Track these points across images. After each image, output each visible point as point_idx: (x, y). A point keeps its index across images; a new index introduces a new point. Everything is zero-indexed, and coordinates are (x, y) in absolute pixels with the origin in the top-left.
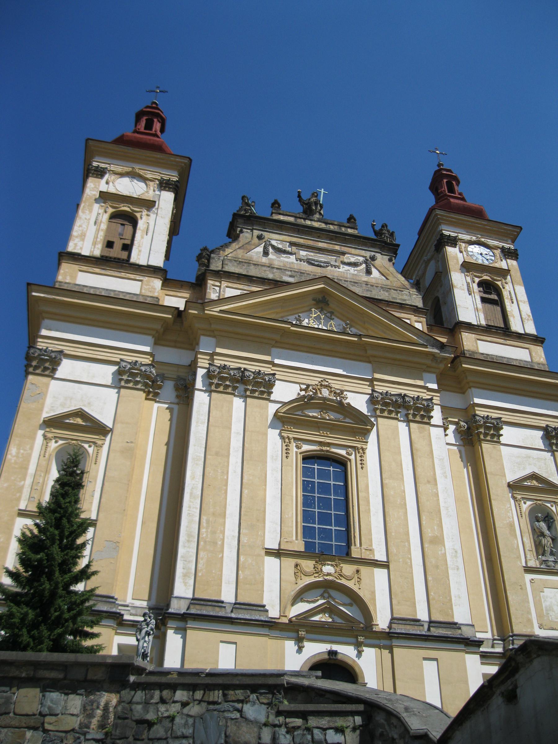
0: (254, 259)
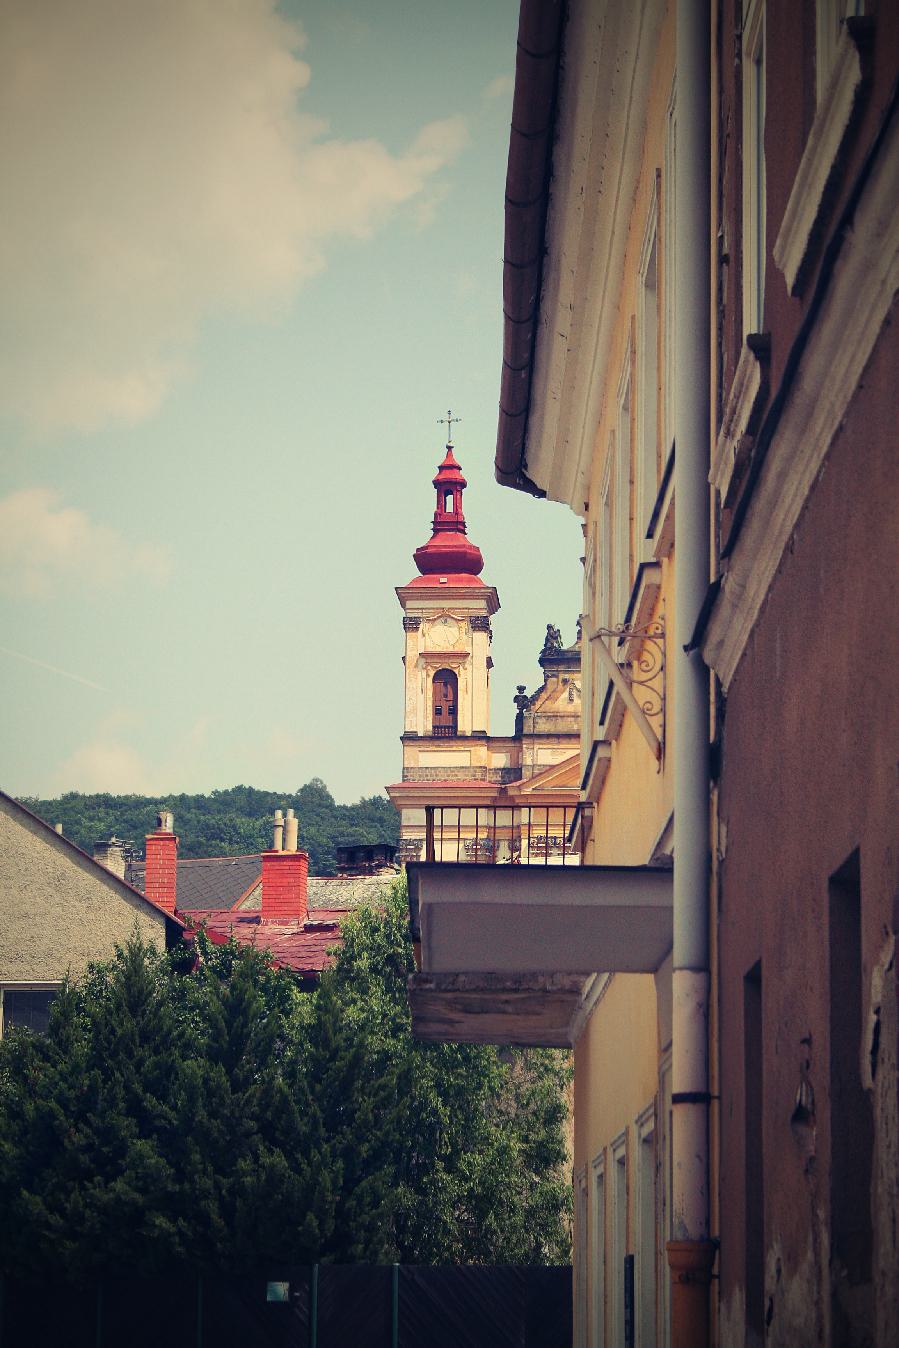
0: (561, 710)
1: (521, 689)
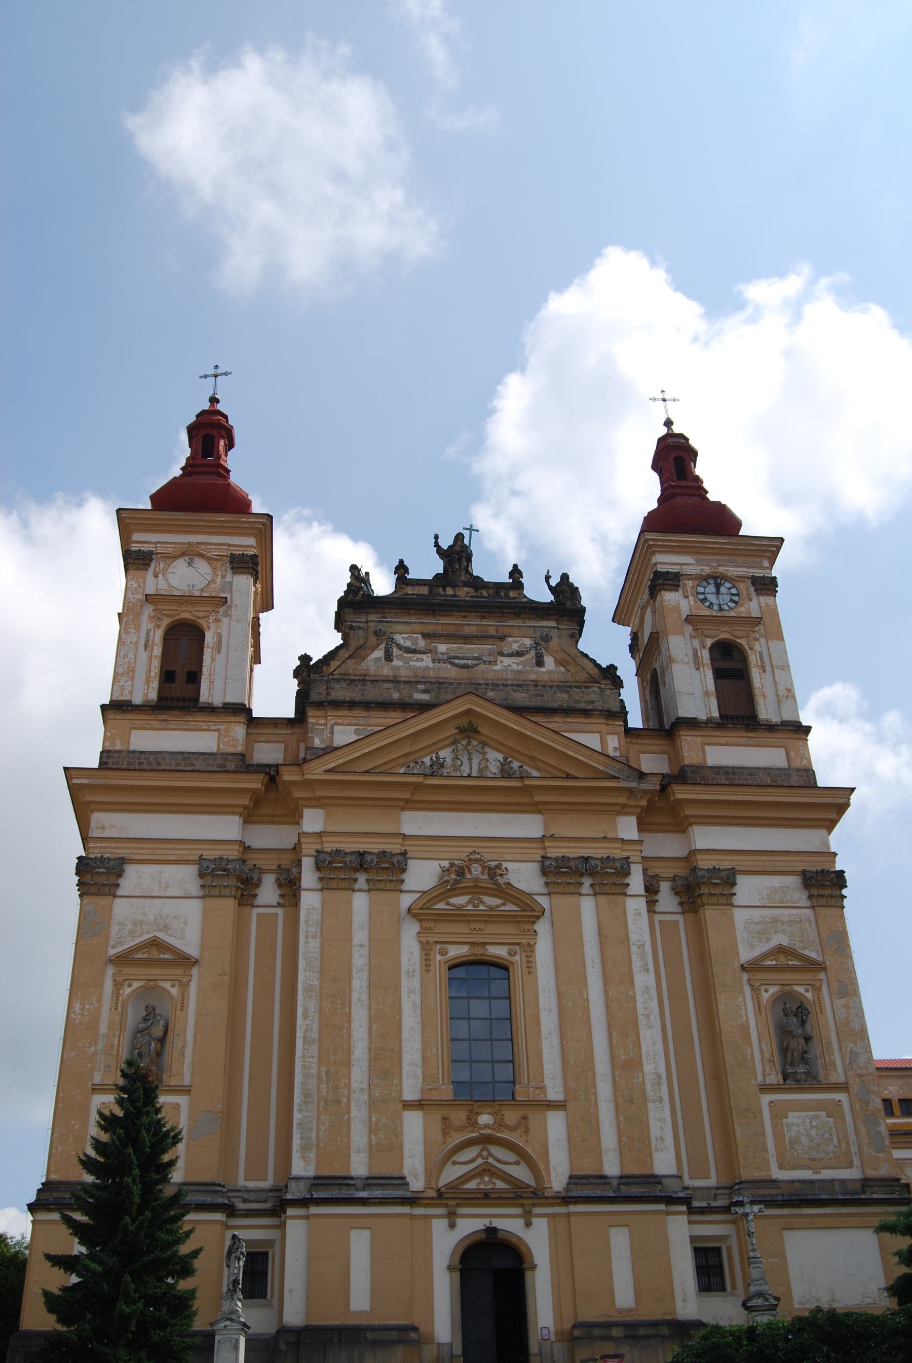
0: (372, 672)
1: (305, 659)
